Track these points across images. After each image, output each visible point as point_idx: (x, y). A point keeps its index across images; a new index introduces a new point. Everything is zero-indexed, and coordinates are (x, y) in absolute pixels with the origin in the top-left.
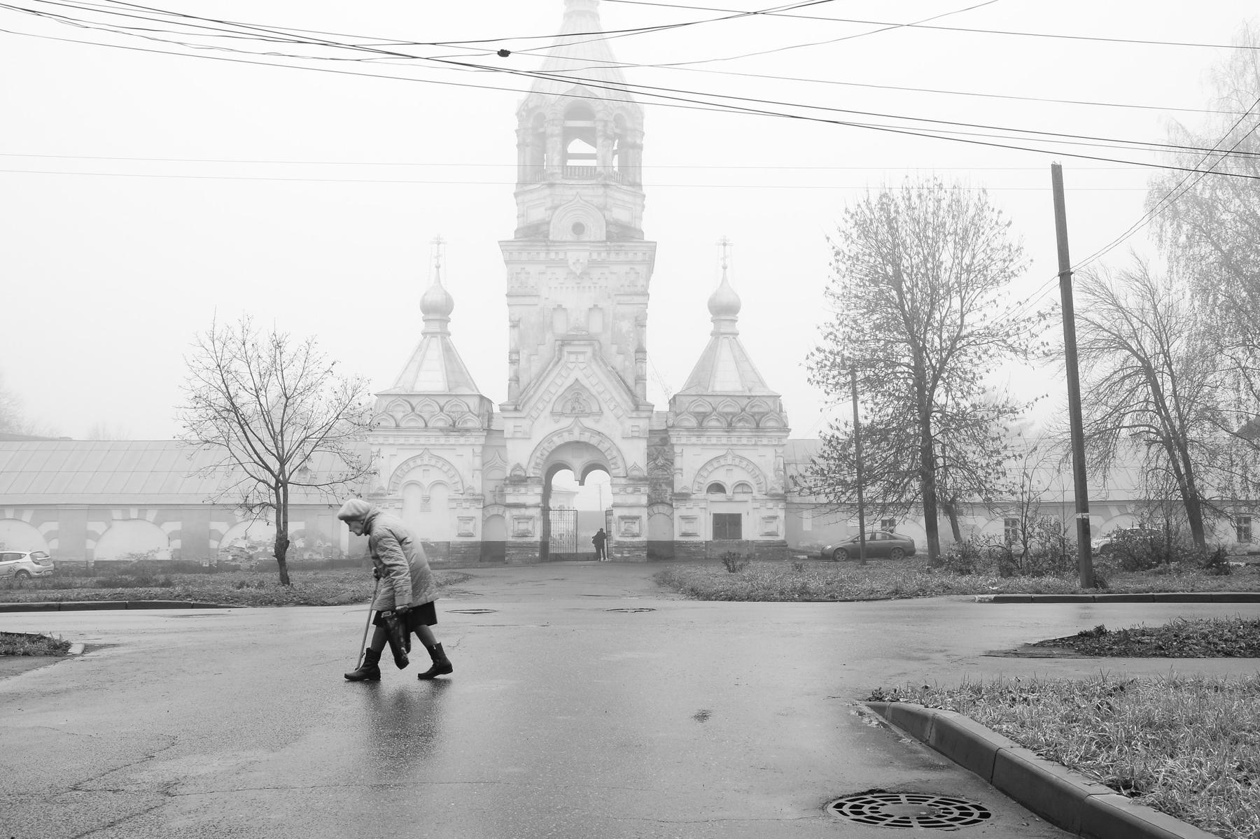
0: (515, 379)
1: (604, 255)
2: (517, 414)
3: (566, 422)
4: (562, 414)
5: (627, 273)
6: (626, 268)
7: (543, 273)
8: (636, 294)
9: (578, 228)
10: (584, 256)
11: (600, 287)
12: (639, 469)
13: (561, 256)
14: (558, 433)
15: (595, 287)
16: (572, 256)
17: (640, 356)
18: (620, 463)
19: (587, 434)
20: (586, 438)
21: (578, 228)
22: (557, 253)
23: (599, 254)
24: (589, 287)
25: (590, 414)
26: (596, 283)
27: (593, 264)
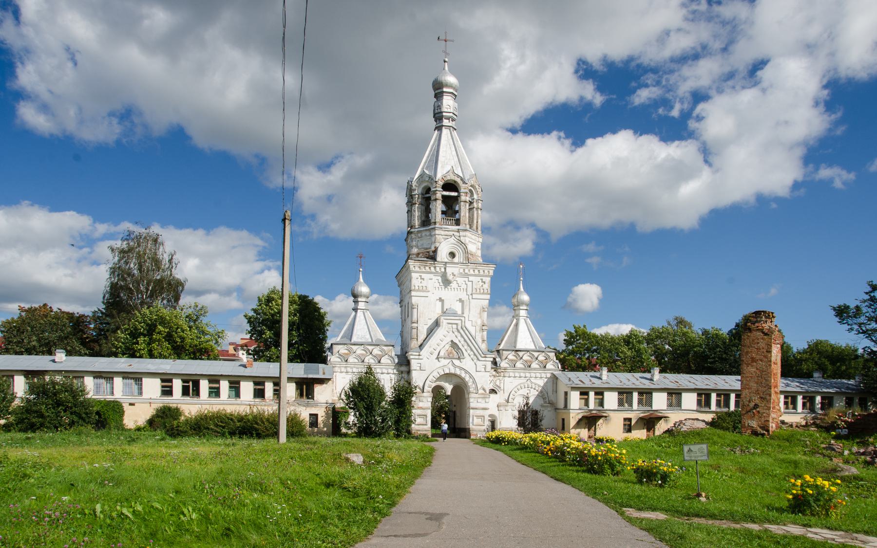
2: (421, 357)
6: (479, 279)
9: (452, 255)
21: (452, 255)
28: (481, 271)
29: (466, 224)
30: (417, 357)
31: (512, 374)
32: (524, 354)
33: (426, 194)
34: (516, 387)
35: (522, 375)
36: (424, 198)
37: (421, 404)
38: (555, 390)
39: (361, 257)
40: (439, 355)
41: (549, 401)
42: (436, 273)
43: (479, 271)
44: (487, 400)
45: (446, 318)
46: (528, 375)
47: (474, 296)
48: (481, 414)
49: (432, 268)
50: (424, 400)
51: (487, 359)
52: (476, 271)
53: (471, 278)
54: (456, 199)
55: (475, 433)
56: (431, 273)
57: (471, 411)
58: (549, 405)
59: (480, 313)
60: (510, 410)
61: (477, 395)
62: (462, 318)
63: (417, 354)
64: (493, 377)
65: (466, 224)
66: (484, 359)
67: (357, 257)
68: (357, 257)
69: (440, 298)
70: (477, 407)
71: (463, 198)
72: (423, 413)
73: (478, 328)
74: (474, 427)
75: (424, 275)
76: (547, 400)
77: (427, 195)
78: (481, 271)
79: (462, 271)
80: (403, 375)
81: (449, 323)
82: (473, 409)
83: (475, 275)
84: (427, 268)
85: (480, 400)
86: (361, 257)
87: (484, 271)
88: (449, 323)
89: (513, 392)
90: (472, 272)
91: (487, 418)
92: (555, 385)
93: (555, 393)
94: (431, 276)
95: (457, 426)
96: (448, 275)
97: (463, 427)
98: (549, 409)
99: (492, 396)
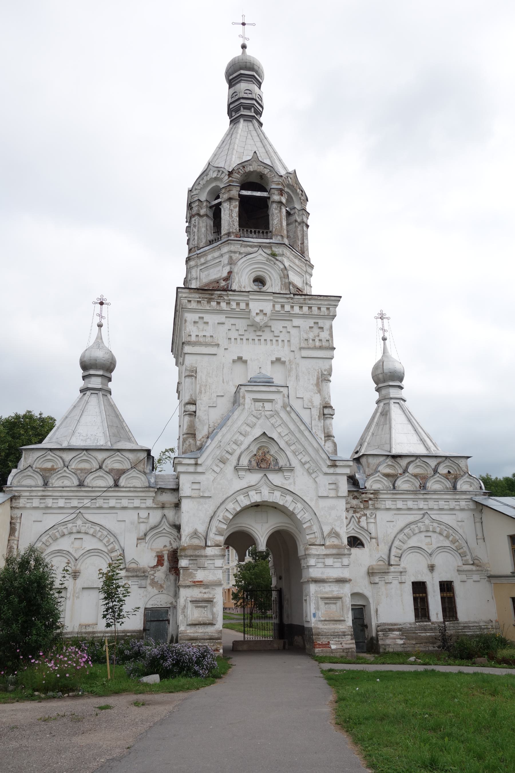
0: (191, 434)
1: (287, 308)
2: (200, 469)
3: (254, 478)
4: (250, 470)
5: (311, 328)
6: (311, 322)
7: (223, 324)
8: (321, 348)
9: (259, 281)
10: (267, 307)
11: (283, 341)
12: (337, 535)
13: (243, 306)
14: (245, 491)
15: (277, 341)
16: (255, 307)
17: (326, 411)
18: (315, 528)
19: (277, 494)
20: (277, 498)
21: (259, 281)
22: (238, 304)
23: (283, 306)
24: (271, 340)
25: (280, 470)
26: (279, 336)
27: (276, 316)
28: (315, 309)
29: (282, 236)
30: (191, 469)
31: (389, 504)
32: (409, 464)
33: (216, 199)
34: (402, 530)
35: (410, 504)
36: (211, 207)
37: (200, 575)
38: (480, 536)
39: (102, 303)
40: (239, 460)
41: (474, 559)
42: (231, 314)
43: (310, 308)
44: (346, 561)
45: (250, 388)
46: (422, 504)
47: (305, 353)
48: (335, 594)
49: (223, 305)
50: (208, 563)
51: (339, 470)
52: (305, 309)
53: (296, 322)
54: (264, 203)
55: (324, 640)
56: (221, 312)
57: (313, 588)
58: (474, 568)
59: (317, 385)
60: (395, 582)
61: (322, 550)
62: (281, 389)
63: (192, 461)
64: (351, 512)
65: (282, 236)
66: (331, 470)
67: (96, 303)
68: (96, 303)
69: (240, 359)
70: (324, 576)
71: (276, 197)
72: (206, 596)
73: (316, 413)
74: (320, 626)
75: (207, 317)
76: (468, 557)
77: (217, 202)
78: (315, 309)
79: (278, 307)
80: (166, 512)
81: (256, 400)
82: (316, 581)
83: (304, 316)
84: (214, 304)
85: (329, 561)
86: (102, 303)
87: (319, 308)
88: (256, 400)
89: (397, 543)
90: (296, 309)
91: (348, 602)
92: (478, 525)
93: (480, 541)
94: (222, 318)
95: (286, 621)
96: (253, 314)
97: (296, 622)
98: (476, 577)
99: (355, 551)
